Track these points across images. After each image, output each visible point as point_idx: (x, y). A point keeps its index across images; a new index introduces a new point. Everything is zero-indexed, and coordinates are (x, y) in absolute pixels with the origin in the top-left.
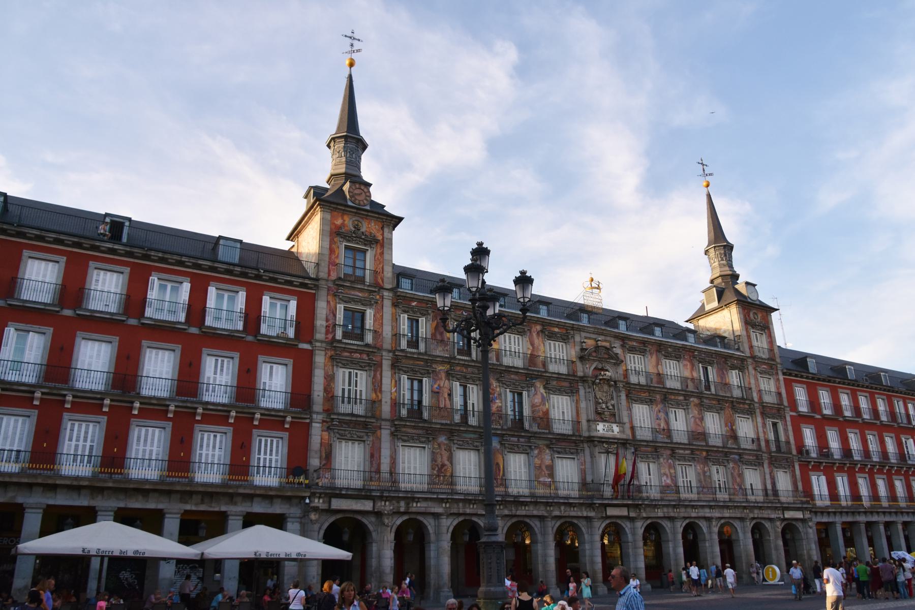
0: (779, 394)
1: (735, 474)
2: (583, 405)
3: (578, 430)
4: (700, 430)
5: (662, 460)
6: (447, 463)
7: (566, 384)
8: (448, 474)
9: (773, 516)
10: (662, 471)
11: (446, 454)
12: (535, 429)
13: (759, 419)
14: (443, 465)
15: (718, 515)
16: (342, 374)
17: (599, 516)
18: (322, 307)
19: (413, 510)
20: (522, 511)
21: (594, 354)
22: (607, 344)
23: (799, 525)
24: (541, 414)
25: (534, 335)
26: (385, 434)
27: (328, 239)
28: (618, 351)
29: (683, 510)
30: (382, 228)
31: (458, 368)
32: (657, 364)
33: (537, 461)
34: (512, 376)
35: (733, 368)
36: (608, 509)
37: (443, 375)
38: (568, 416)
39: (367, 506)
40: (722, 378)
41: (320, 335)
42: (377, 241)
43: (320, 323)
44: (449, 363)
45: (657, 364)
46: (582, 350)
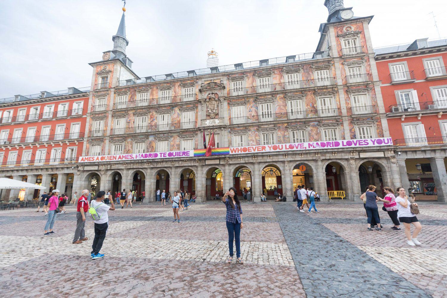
0: (370, 75)
1: (314, 133)
2: (199, 113)
3: (196, 126)
5: (250, 133)
6: (130, 149)
7: (192, 106)
9: (347, 157)
10: (250, 139)
11: (130, 146)
12: (173, 129)
13: (342, 95)
15: (289, 159)
17: (201, 164)
18: (90, 101)
20: (159, 165)
21: (208, 87)
23: (384, 163)
25: (177, 87)
26: (107, 142)
27: (94, 77)
29: (260, 158)
31: (139, 111)
32: (253, 82)
33: (172, 143)
34: (163, 108)
35: (318, 69)
36: (206, 161)
37: (132, 115)
38: (193, 119)
39: (96, 168)
41: (89, 111)
42: (111, 71)
43: (90, 107)
45: (253, 82)
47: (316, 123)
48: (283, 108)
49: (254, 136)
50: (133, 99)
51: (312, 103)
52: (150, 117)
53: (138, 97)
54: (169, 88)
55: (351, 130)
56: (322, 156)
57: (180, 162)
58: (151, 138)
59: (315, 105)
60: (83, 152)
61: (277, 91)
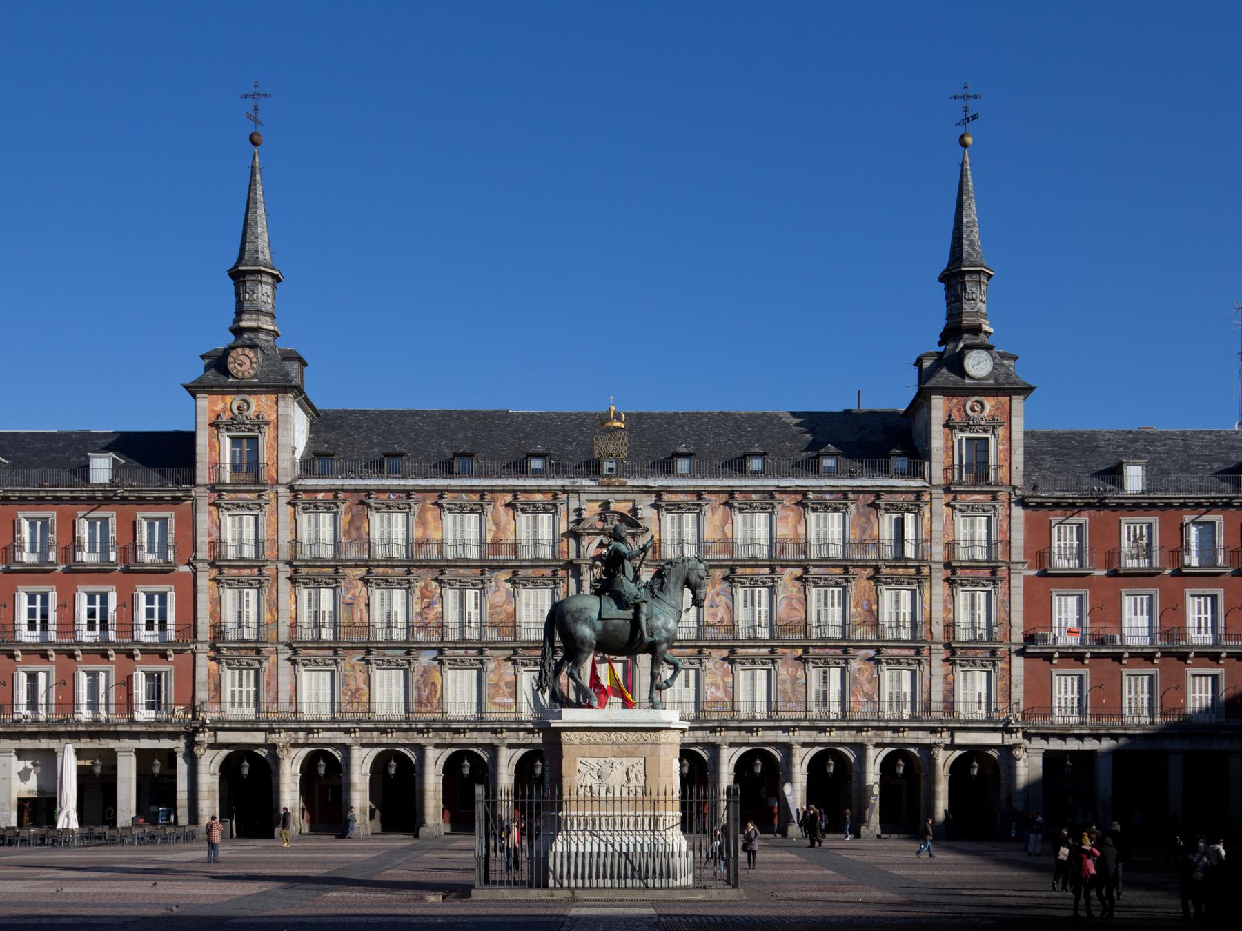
4: (798, 616)
8: (365, 699)
11: (361, 677)
12: (492, 635)
13: (940, 589)
14: (358, 690)
15: (802, 740)
16: (229, 595)
18: (204, 519)
19: (315, 741)
22: (624, 507)
24: (503, 616)
28: (647, 513)
30: (277, 403)
39: (259, 738)
40: (864, 530)
41: (203, 553)
43: (203, 540)
44: (366, 566)
45: (725, 523)
46: (579, 521)
47: (872, 653)
48: (799, 606)
49: (719, 673)
50: (358, 529)
51: (869, 600)
52: (417, 592)
53: (377, 524)
54: (478, 510)
55: (946, 677)
56: (876, 735)
57: (522, 734)
58: (425, 659)
59: (874, 607)
60: (198, 687)
61: (787, 560)
